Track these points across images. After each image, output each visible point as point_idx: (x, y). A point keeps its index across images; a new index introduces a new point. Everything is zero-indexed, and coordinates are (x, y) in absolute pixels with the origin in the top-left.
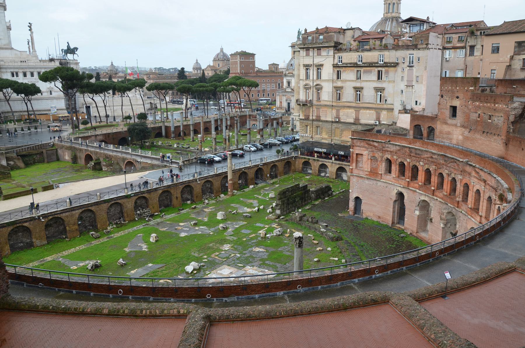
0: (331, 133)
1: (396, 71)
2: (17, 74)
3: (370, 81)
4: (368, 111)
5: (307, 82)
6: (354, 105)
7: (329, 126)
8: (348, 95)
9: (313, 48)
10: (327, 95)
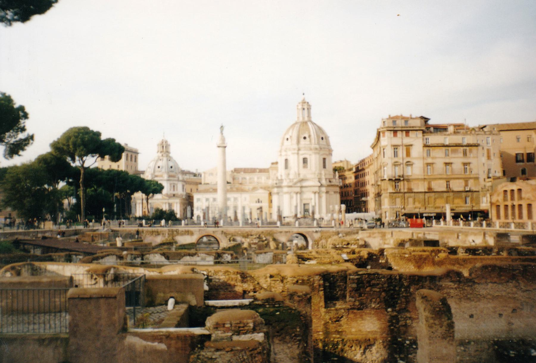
1: (478, 150)
3: (457, 157)
5: (396, 159)
6: (445, 177)
7: (421, 196)
9: (402, 131)
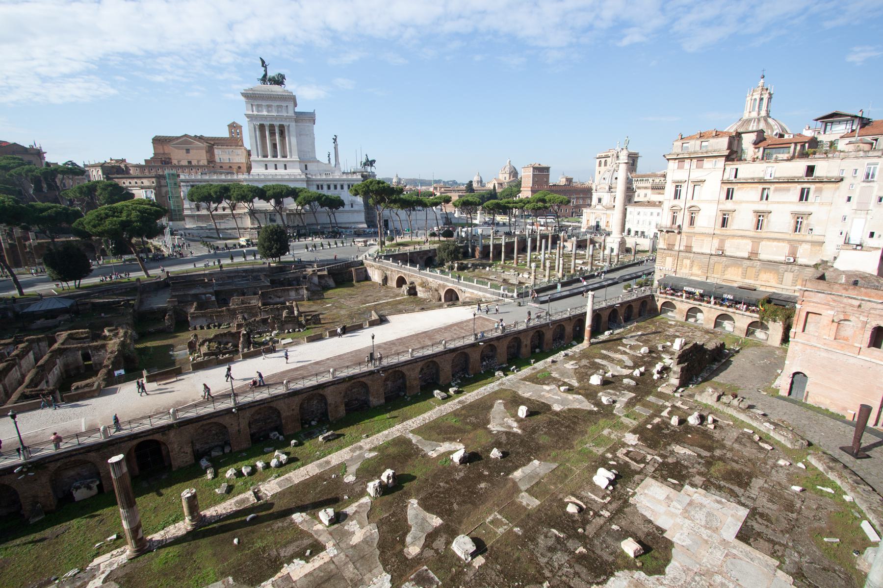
0: (708, 268)
1: (838, 188)
2: (322, 186)
3: (784, 203)
4: (775, 243)
8: (743, 220)
9: (691, 159)
10: (707, 220)
